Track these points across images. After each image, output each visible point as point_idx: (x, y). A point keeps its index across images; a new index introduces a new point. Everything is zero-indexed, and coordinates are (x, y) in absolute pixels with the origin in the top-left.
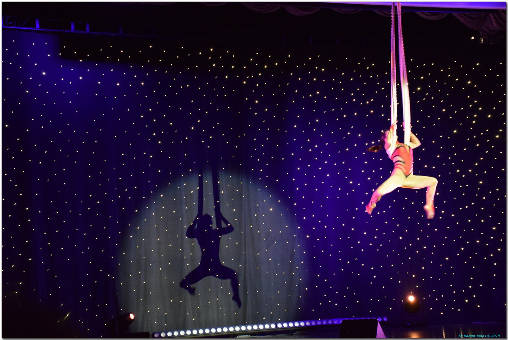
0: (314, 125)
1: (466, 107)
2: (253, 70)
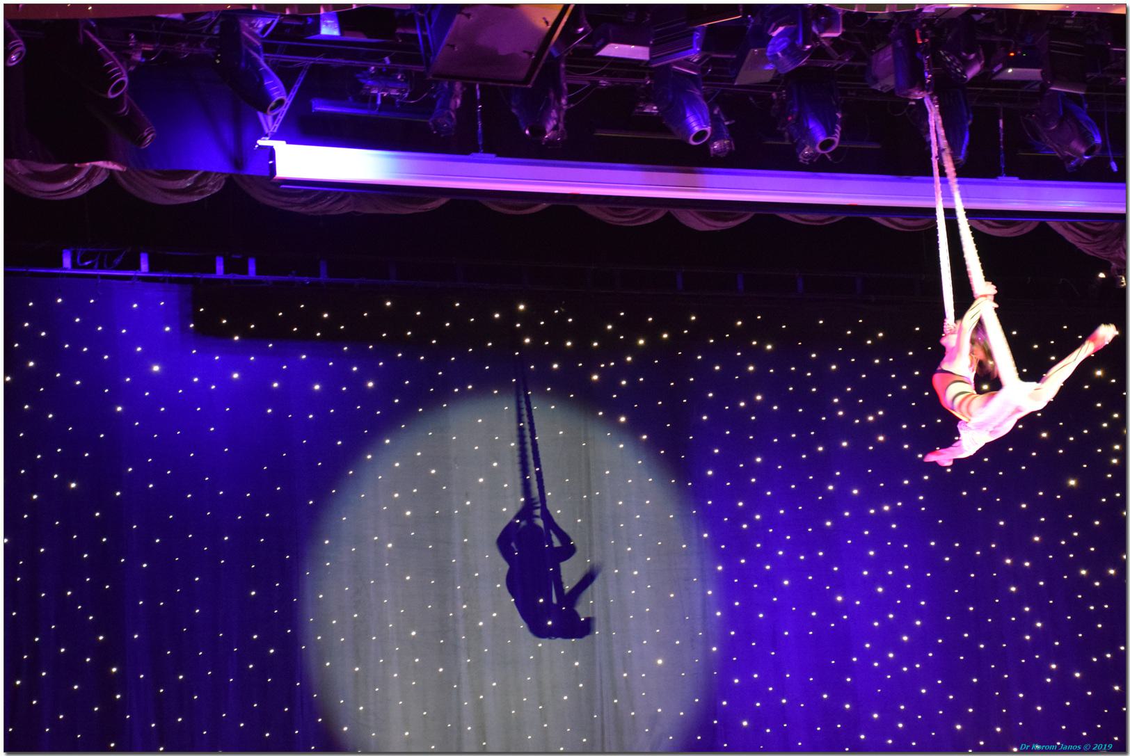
0: (752, 469)
2: (613, 349)
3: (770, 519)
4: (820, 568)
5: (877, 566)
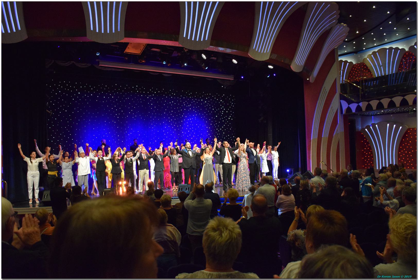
0: (171, 113)
2: (151, 93)
3: (173, 120)
5: (188, 128)
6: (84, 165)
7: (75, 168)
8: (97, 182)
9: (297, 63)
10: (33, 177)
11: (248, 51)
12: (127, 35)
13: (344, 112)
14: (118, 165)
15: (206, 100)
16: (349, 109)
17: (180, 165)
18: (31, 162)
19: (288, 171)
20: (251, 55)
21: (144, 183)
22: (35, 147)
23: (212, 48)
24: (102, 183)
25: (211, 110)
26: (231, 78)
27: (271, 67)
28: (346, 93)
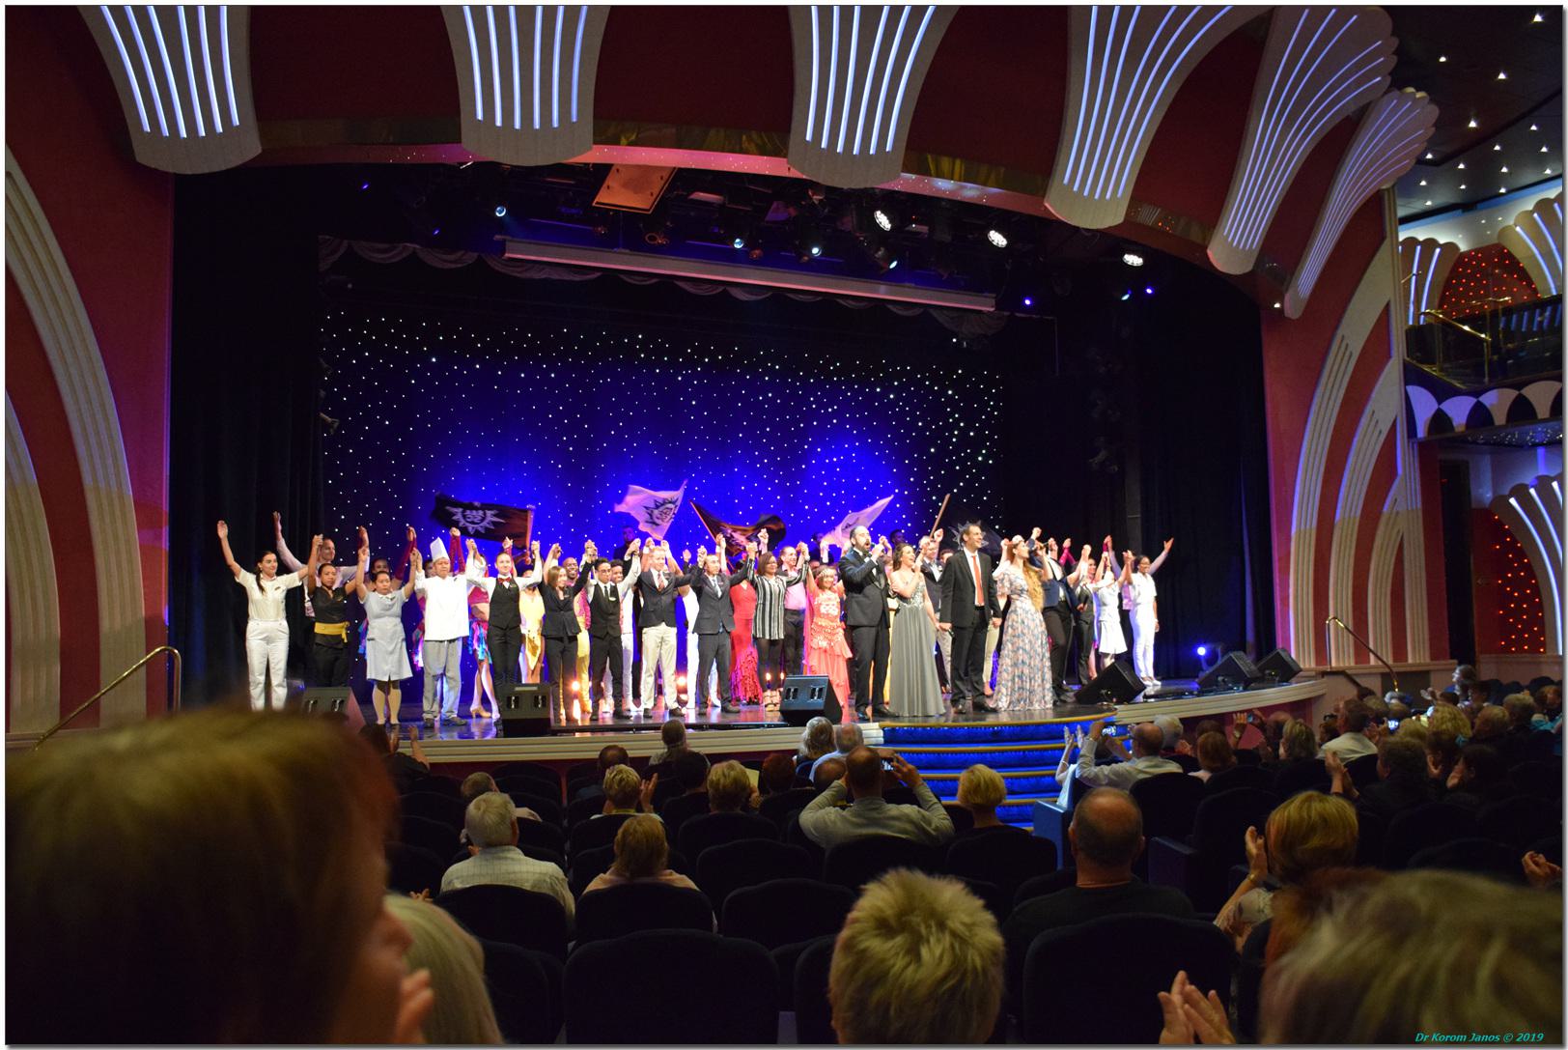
0: (764, 434)
1: (946, 422)
2: (690, 363)
3: (773, 461)
4: (798, 490)
5: (827, 491)
6: (449, 602)
7: (413, 614)
8: (492, 669)
9: (1235, 241)
10: (268, 640)
11: (1041, 191)
12: (603, 135)
13: (1422, 432)
14: (567, 605)
15: (893, 389)
16: (1440, 420)
17: (794, 619)
18: (261, 588)
19: (1202, 651)
20: (1055, 206)
21: (659, 690)
22: (275, 539)
23: (907, 182)
24: (506, 671)
25: (913, 426)
26: (986, 305)
27: (1133, 260)
28: (1432, 363)
